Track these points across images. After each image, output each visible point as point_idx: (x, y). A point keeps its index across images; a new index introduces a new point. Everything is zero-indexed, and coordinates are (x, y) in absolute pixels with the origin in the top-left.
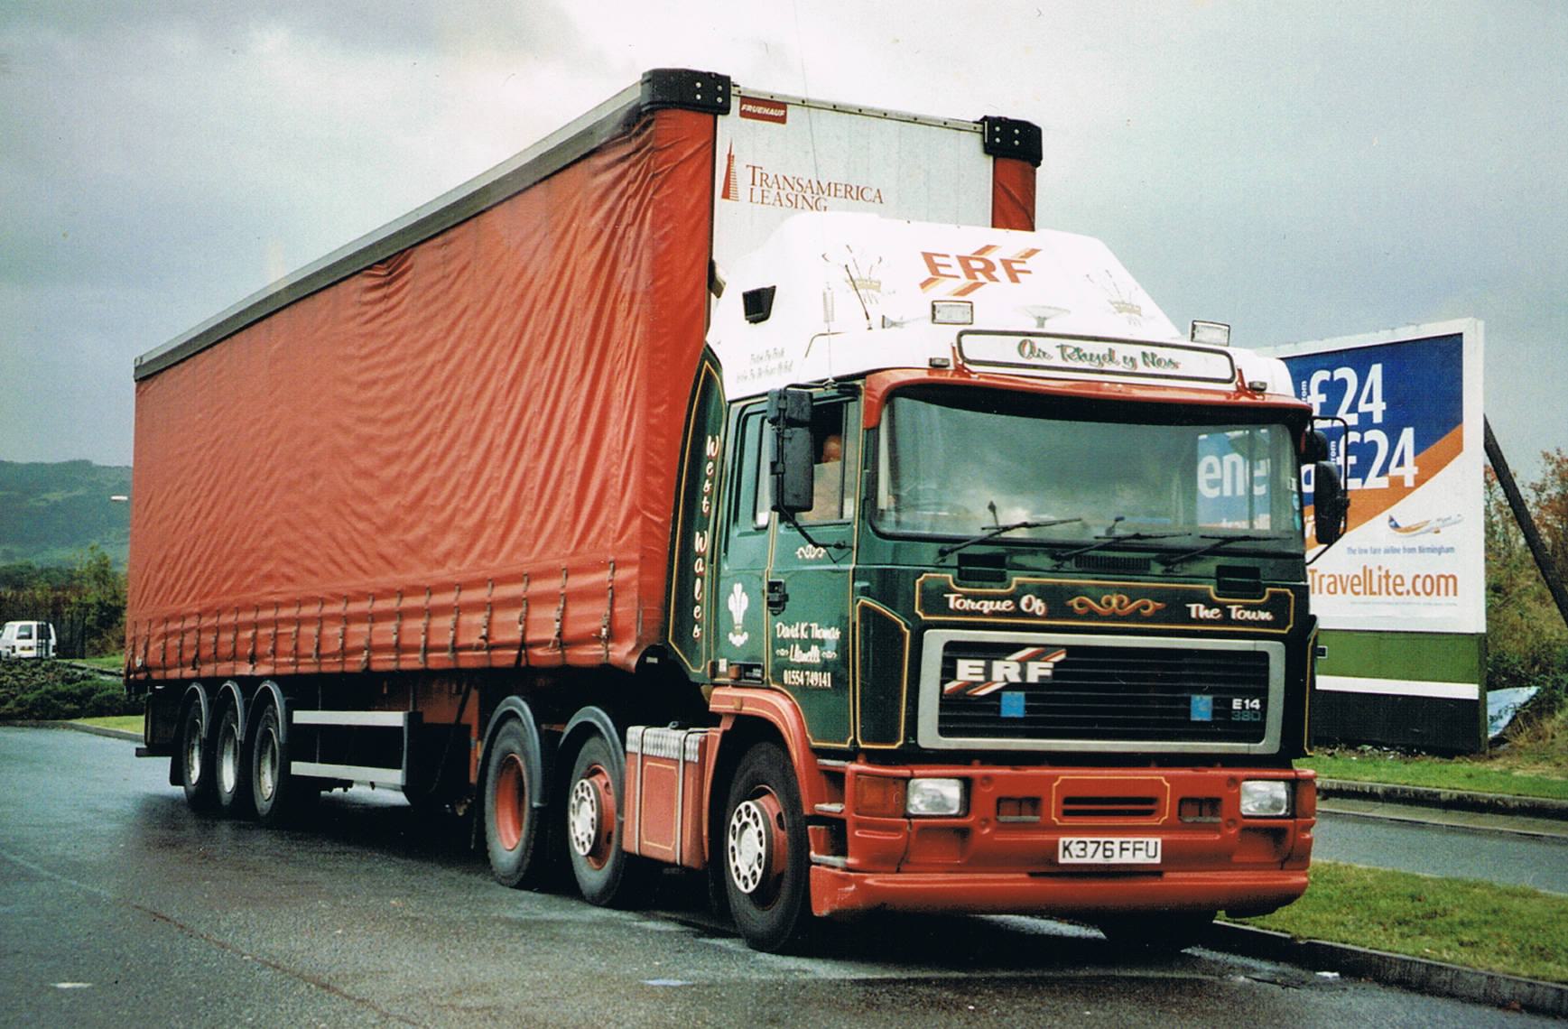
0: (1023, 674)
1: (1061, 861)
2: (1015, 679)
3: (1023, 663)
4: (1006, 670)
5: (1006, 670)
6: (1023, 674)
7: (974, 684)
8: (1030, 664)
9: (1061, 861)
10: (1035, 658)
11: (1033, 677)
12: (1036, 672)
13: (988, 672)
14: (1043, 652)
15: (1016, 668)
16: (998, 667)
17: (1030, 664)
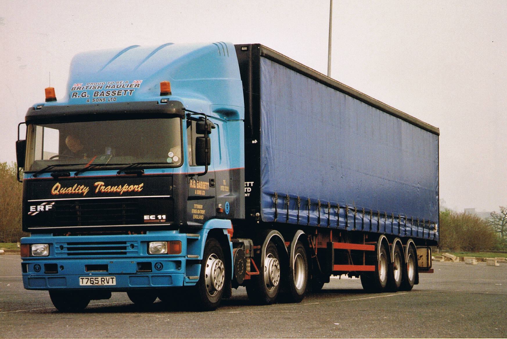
0: (45, 208)
1: (81, 284)
2: (42, 210)
3: (45, 206)
4: (40, 208)
5: (40, 208)
6: (45, 208)
7: (34, 212)
8: (47, 206)
9: (81, 284)
10: (47, 204)
11: (47, 209)
12: (48, 208)
13: (36, 208)
14: (49, 203)
15: (43, 207)
16: (39, 207)
17: (47, 206)
